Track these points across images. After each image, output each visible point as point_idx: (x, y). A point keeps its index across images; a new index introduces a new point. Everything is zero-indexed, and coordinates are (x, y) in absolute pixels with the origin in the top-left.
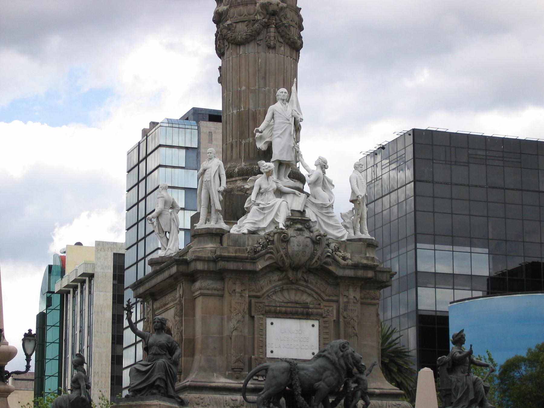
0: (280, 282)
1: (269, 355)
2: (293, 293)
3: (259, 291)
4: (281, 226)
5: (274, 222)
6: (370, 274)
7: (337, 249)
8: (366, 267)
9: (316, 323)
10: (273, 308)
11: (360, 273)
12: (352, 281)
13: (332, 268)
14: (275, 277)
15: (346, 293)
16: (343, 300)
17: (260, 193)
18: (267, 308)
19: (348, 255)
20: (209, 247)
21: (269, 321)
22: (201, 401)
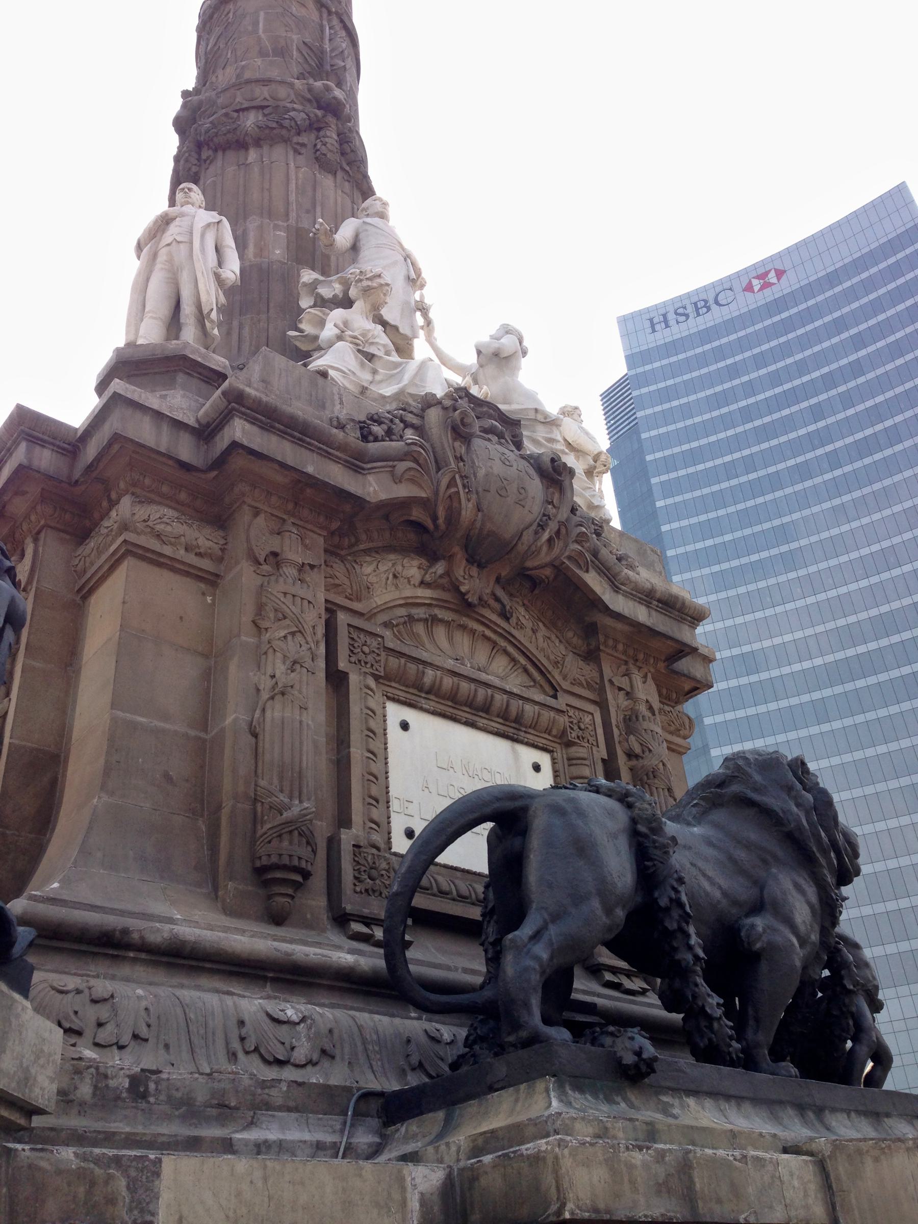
0: (428, 593)
2: (463, 642)
3: (359, 600)
10: (412, 668)
13: (593, 580)
15: (624, 682)
18: (394, 662)
20: (181, 402)
22: (92, 1013)
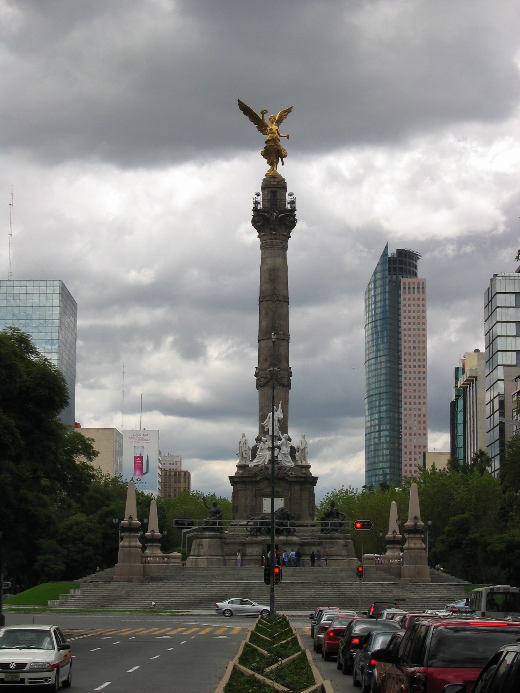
1: (264, 512)
4: (266, 464)
5: (264, 461)
6: (303, 480)
7: (289, 471)
8: (301, 477)
9: (283, 499)
11: (299, 479)
12: (297, 482)
14: (266, 482)
16: (293, 490)
17: (262, 450)
19: (293, 473)
21: (264, 499)
